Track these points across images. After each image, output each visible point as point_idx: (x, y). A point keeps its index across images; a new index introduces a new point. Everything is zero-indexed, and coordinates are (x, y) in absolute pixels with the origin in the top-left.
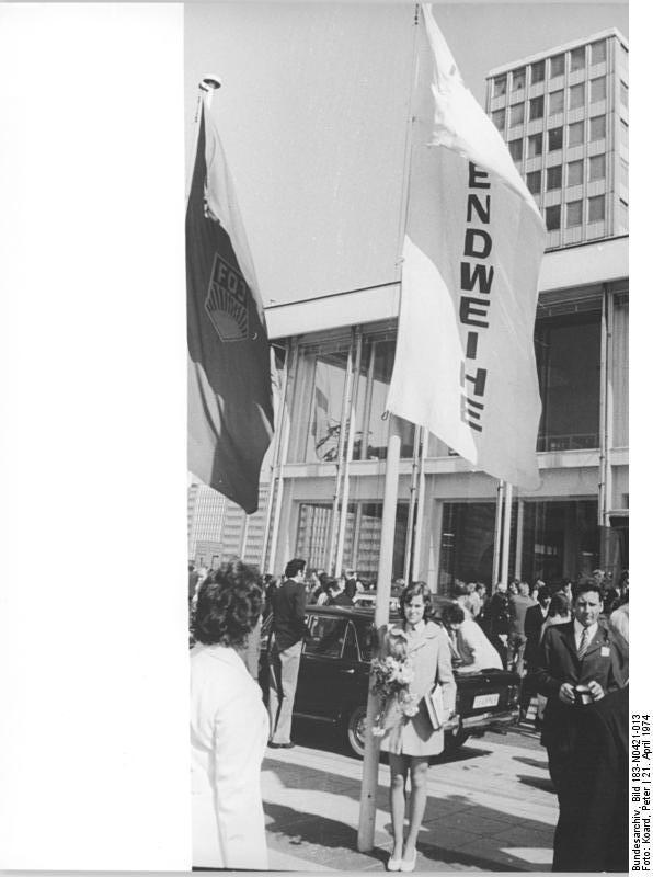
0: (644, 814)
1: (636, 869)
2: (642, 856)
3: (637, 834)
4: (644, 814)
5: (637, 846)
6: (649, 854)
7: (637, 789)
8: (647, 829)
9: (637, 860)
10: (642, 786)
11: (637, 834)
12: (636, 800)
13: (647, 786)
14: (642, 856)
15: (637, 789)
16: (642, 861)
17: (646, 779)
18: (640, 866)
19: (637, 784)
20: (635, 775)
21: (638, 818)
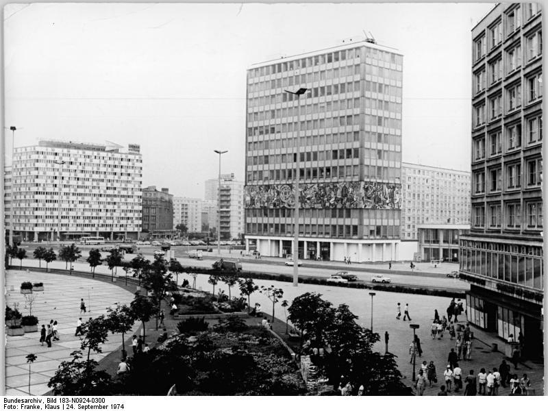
0: (42, 406)
1: (5, 400)
2: (13, 404)
3: (27, 401)
4: (42, 406)
5: (19, 401)
6: (14, 408)
7: (55, 401)
8: (29, 408)
9: (11, 401)
10: (58, 403)
11: (27, 401)
12: (48, 400)
13: (61, 407)
14: (13, 404)
15: (55, 401)
16: (10, 404)
17: (66, 407)
18: (7, 403)
19: (58, 401)
20: (64, 400)
21: (37, 402)
